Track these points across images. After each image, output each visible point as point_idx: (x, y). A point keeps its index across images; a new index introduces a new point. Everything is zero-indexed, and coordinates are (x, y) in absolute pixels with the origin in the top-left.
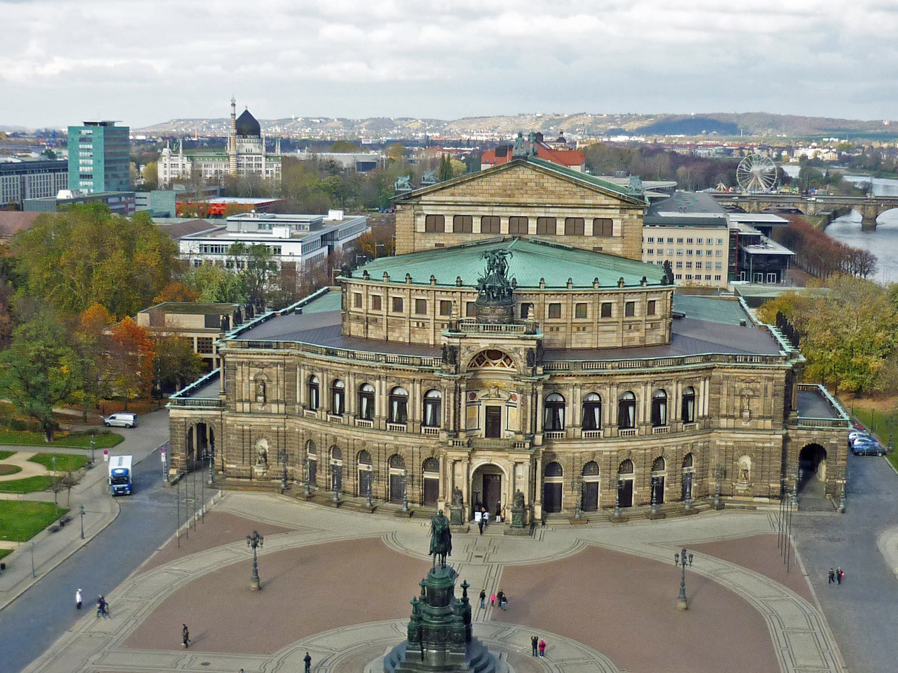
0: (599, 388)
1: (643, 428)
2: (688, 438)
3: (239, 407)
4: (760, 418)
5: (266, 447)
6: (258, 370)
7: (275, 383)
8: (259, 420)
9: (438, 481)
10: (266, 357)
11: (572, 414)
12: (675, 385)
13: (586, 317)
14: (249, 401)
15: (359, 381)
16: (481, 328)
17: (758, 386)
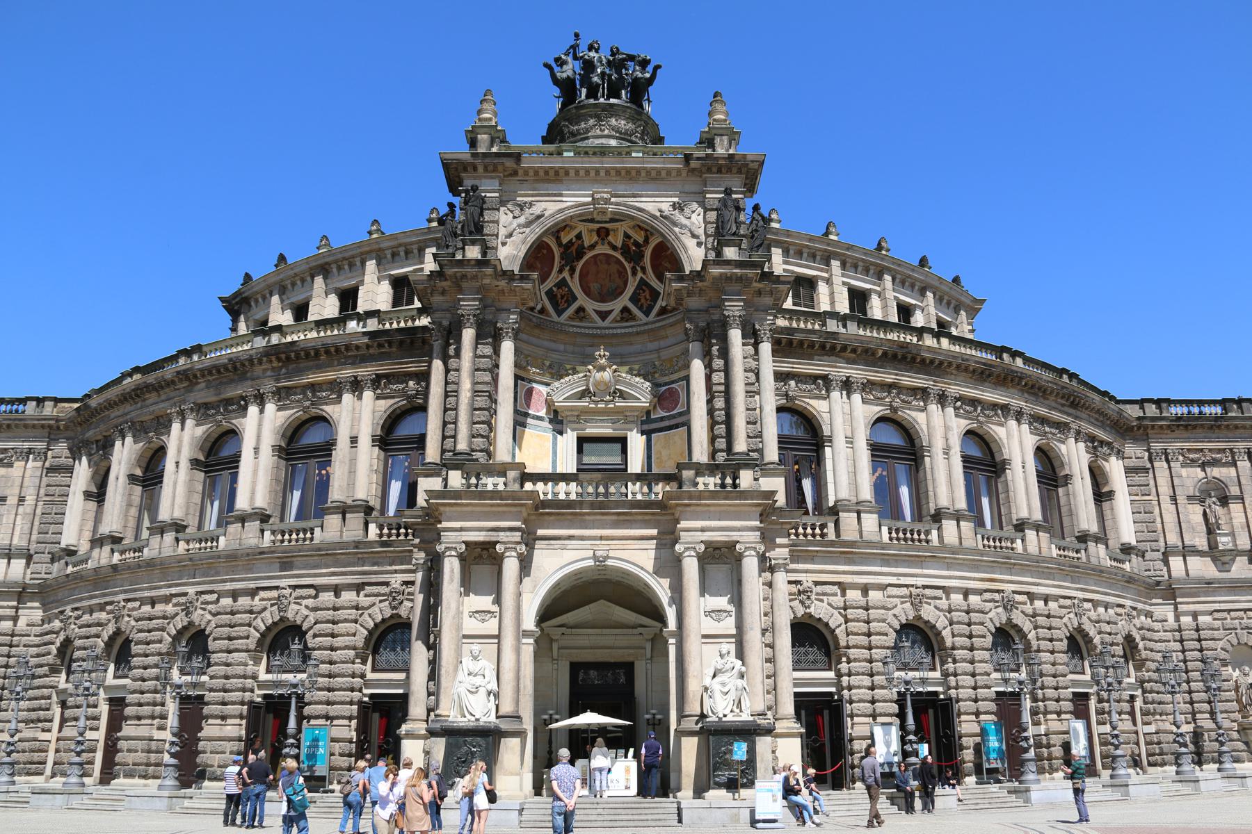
1: (1031, 534)
11: (848, 470)
17: (1233, 470)
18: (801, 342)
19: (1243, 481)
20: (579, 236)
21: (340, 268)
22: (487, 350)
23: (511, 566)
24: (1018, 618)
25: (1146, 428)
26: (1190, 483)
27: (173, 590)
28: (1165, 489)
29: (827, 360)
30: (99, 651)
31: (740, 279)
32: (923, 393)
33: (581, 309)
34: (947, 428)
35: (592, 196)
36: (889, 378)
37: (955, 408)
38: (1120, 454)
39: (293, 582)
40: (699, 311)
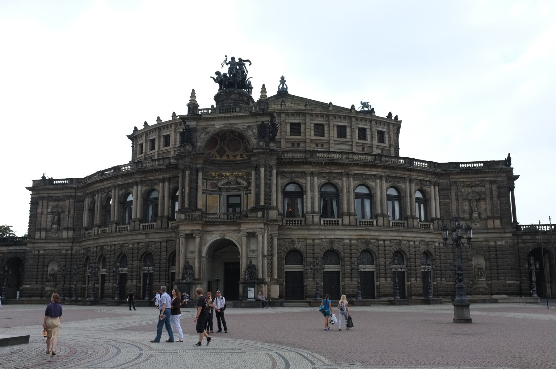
0: (334, 178)
1: (380, 220)
2: (423, 235)
3: (37, 235)
4: (488, 218)
5: (56, 268)
6: (55, 203)
7: (67, 213)
8: (52, 245)
10: (62, 192)
11: (312, 201)
12: (408, 183)
13: (323, 136)
14: (46, 230)
17: (483, 189)
18: (296, 162)
19: (487, 193)
20: (225, 134)
21: (164, 128)
22: (194, 177)
23: (198, 240)
24: (370, 247)
25: (448, 174)
26: (465, 194)
27: (116, 243)
28: (453, 196)
29: (305, 166)
31: (262, 153)
33: (228, 155)
35: (224, 124)
39: (148, 240)
40: (254, 161)
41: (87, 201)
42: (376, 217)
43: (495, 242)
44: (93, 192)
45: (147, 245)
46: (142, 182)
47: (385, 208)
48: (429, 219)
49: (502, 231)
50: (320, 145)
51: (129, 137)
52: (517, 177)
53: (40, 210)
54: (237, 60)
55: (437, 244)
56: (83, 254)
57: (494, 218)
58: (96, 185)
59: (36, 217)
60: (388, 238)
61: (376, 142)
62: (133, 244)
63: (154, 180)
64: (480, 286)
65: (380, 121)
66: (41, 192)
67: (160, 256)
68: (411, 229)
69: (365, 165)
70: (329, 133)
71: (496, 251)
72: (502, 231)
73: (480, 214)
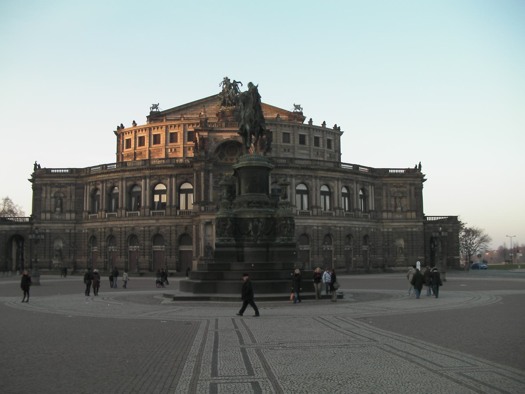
0: (307, 179)
1: (338, 211)
2: (364, 223)
3: (43, 216)
4: (408, 211)
5: (61, 245)
6: (57, 189)
7: (68, 198)
8: (56, 225)
9: (191, 251)
10: (63, 179)
12: (355, 184)
13: (289, 142)
14: (50, 212)
15: (130, 183)
16: (224, 124)
17: (405, 190)
18: (280, 167)
21: (154, 129)
27: (127, 225)
28: (384, 194)
29: (287, 170)
30: (106, 240)
32: (311, 176)
33: (226, 159)
34: (316, 186)
36: (303, 174)
37: (320, 180)
38: (372, 184)
41: (89, 189)
42: (335, 209)
43: (412, 229)
44: (97, 181)
45: (158, 228)
46: (150, 176)
47: (340, 203)
48: (366, 210)
49: (417, 221)
50: (287, 150)
51: (115, 132)
52: (426, 180)
53: (44, 195)
54: (232, 82)
55: (372, 230)
56: (88, 233)
57: (411, 211)
58: (101, 176)
59: (40, 201)
60: (342, 225)
61: (326, 148)
62: (144, 227)
63: (161, 175)
64: (400, 260)
65: (329, 131)
66: (44, 179)
67: (170, 237)
68: (357, 218)
69: (329, 170)
70: (294, 141)
71: (412, 235)
72: (417, 221)
73: (402, 209)
